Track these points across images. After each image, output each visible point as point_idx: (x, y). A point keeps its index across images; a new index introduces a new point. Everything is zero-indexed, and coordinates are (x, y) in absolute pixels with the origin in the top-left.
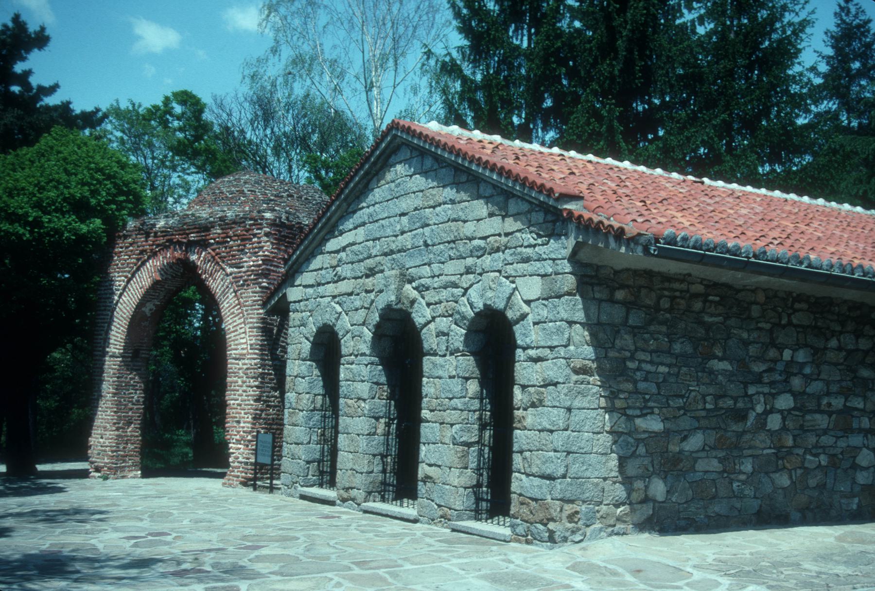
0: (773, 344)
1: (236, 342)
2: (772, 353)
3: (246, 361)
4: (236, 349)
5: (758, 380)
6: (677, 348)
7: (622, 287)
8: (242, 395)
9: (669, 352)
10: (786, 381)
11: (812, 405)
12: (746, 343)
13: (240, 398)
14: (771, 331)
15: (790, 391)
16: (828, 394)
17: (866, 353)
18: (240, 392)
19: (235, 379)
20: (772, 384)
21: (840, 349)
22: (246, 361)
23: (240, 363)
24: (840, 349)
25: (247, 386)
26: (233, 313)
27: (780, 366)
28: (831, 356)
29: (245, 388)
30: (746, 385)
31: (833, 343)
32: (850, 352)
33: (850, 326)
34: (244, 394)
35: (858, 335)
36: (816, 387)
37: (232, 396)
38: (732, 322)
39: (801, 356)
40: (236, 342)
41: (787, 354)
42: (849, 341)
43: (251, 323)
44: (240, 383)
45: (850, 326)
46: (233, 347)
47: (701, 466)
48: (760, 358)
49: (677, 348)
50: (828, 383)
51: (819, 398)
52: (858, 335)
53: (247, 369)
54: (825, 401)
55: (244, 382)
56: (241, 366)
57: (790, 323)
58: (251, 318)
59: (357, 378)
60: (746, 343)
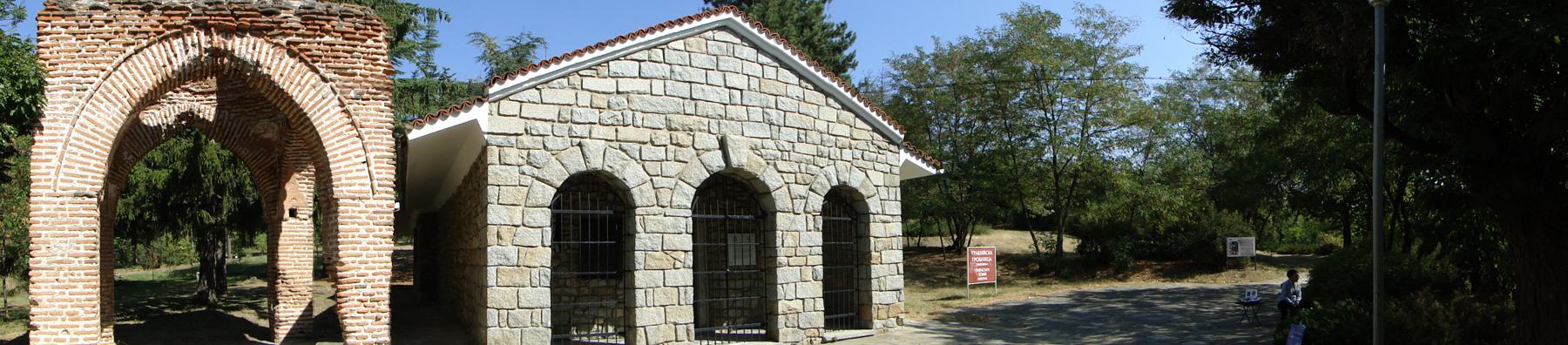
1: (349, 175)
3: (374, 202)
8: (368, 249)
13: (365, 253)
18: (364, 244)
19: (356, 226)
22: (374, 202)
25: (374, 236)
26: (338, 135)
29: (371, 239)
34: (372, 246)
37: (350, 252)
40: (349, 175)
43: (378, 150)
53: (375, 212)
56: (362, 207)
58: (376, 144)
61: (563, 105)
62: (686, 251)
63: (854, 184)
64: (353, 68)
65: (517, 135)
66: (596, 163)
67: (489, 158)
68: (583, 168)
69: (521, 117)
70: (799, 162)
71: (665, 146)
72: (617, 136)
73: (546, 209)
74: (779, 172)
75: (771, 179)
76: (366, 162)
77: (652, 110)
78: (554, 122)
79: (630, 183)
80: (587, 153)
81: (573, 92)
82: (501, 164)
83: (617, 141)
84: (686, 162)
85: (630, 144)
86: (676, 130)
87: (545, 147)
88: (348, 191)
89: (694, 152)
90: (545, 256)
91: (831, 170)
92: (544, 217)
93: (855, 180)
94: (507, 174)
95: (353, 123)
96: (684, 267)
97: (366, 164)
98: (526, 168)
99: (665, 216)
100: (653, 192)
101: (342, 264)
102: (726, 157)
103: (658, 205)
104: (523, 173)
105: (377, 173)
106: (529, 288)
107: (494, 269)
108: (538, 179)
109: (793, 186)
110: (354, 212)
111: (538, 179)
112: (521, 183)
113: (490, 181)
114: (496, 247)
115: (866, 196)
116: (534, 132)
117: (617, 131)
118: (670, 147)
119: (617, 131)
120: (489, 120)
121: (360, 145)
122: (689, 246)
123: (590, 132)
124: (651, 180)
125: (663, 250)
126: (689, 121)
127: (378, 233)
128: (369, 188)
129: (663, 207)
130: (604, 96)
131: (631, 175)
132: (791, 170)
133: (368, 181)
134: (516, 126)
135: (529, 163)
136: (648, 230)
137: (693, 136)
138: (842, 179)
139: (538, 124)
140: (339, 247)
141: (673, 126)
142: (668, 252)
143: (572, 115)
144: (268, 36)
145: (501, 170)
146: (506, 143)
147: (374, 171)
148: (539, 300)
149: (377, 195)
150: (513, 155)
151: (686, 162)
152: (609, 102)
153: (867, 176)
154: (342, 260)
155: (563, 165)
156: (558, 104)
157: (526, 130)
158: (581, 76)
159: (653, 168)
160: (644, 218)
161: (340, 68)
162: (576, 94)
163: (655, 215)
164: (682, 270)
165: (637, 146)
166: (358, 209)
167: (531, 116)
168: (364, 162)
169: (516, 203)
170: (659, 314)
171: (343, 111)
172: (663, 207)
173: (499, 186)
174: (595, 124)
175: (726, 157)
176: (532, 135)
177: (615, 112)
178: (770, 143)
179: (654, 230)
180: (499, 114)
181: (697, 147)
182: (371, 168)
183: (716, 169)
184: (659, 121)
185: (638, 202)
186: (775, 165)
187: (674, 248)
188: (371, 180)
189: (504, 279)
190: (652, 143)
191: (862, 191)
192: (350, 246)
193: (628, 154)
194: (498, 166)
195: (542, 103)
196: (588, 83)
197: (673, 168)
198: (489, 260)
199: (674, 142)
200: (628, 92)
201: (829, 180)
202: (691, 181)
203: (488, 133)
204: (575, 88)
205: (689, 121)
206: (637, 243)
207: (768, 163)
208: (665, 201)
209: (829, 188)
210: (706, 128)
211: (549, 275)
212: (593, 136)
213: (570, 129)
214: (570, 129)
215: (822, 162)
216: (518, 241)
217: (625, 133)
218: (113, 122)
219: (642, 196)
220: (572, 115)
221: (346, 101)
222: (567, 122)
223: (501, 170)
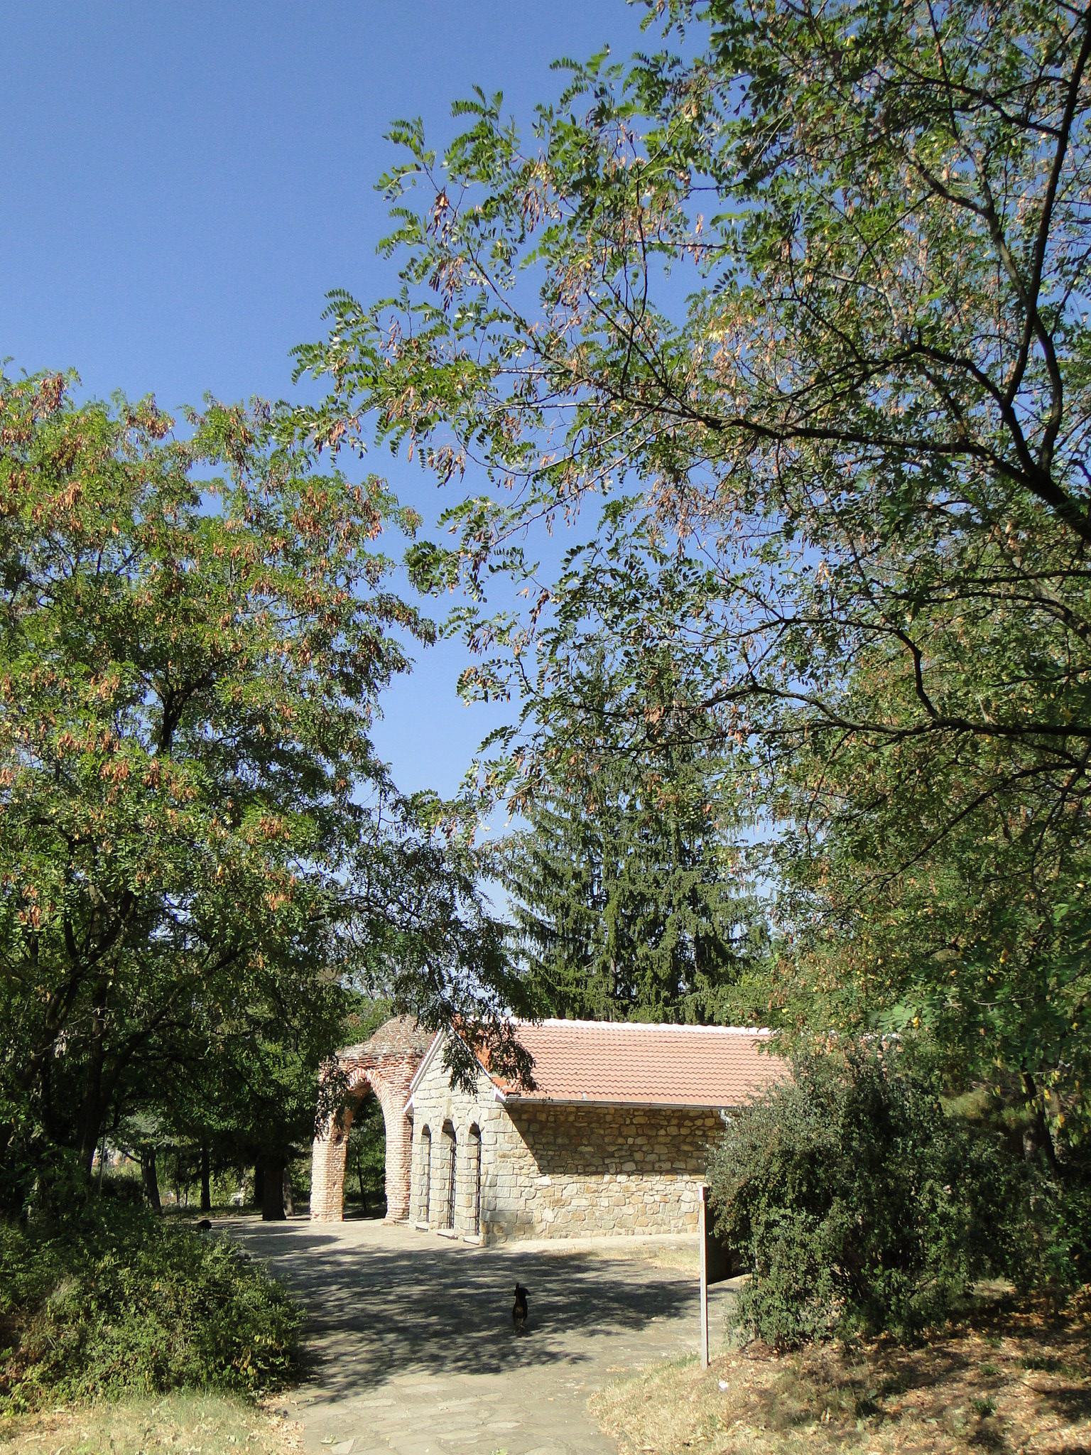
0: (620, 1135)
2: (620, 1140)
5: (612, 1155)
6: (559, 1141)
7: (526, 1112)
9: (555, 1144)
10: (631, 1155)
11: (649, 1167)
12: (603, 1136)
14: (619, 1128)
15: (633, 1161)
16: (660, 1161)
17: (686, 1136)
20: (620, 1157)
21: (667, 1135)
24: (667, 1135)
27: (625, 1147)
28: (661, 1139)
30: (603, 1159)
31: (662, 1132)
32: (674, 1137)
33: (674, 1122)
35: (679, 1126)
36: (652, 1157)
38: (593, 1125)
39: (639, 1141)
41: (630, 1141)
42: (673, 1130)
45: (674, 1122)
47: (575, 1202)
48: (613, 1144)
49: (559, 1141)
50: (659, 1155)
51: (654, 1164)
52: (679, 1126)
54: (657, 1165)
57: (632, 1123)
60: (603, 1136)
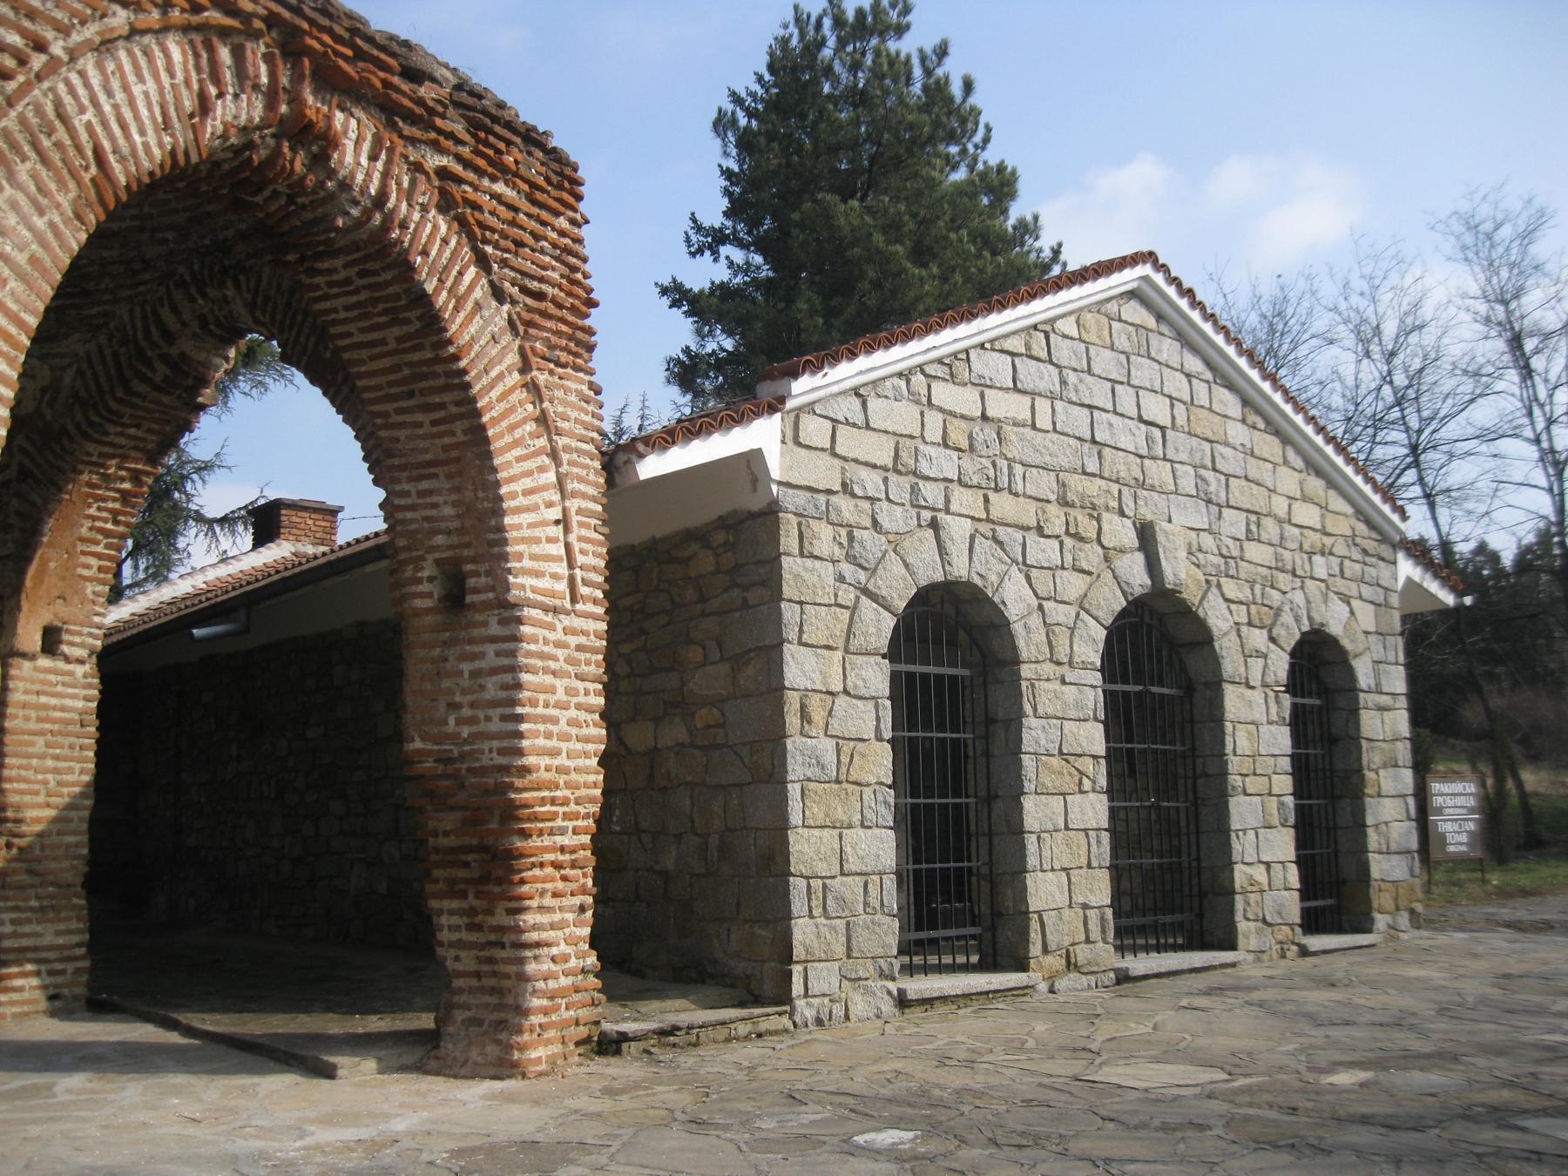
4: (538, 574)
23: (559, 627)
29: (573, 713)
37: (541, 742)
44: (561, 695)
46: (527, 563)
53: (580, 648)
55: (570, 692)
56: (558, 635)
59: (1072, 714)
61: (901, 435)
62: (1094, 757)
63: (1335, 629)
64: (541, 280)
65: (829, 492)
66: (960, 568)
67: (782, 540)
68: (939, 577)
69: (835, 455)
70: (1252, 583)
71: (1057, 537)
72: (987, 511)
73: (879, 659)
74: (1227, 600)
75: (1217, 617)
76: (564, 522)
77: (1037, 462)
78: (886, 469)
79: (1013, 611)
80: (948, 544)
81: (915, 410)
82: (802, 554)
83: (988, 520)
84: (1089, 573)
85: (1009, 530)
86: (1072, 506)
87: (875, 523)
88: (534, 590)
89: (1100, 551)
90: (879, 763)
91: (1298, 597)
92: (876, 677)
93: (1335, 619)
94: (815, 579)
95: (542, 420)
96: (1094, 790)
97: (561, 527)
98: (847, 569)
99: (1063, 682)
100: (1043, 631)
101: (525, 770)
102: (1153, 565)
103: (1051, 660)
104: (841, 578)
105: (581, 552)
106: (861, 832)
107: (797, 786)
108: (866, 591)
109: (1244, 629)
110: (546, 641)
111: (866, 591)
112: (840, 600)
113: (788, 590)
114: (799, 739)
115: (1351, 654)
116: (858, 491)
117: (986, 500)
118: (1069, 542)
119: (986, 500)
120: (782, 454)
121: (551, 477)
122: (1100, 747)
123: (947, 501)
124: (1041, 607)
125: (1061, 752)
126: (1094, 487)
127: (581, 699)
128: (562, 587)
129: (1059, 663)
130: (963, 424)
131: (1014, 598)
132: (1241, 597)
133: (562, 569)
134: (824, 473)
135: (852, 559)
136: (1040, 711)
137: (1098, 520)
138: (1318, 618)
139: (863, 473)
140: (524, 727)
141: (1071, 497)
142: (1071, 759)
143: (917, 460)
144: (401, 136)
145: (806, 569)
146: (811, 511)
147: (577, 546)
148: (878, 856)
149: (579, 607)
150: (824, 538)
151: (1089, 573)
152: (970, 437)
153: (1352, 612)
154: (530, 760)
155: (906, 565)
156: (895, 434)
157: (844, 485)
158: (927, 376)
159: (1042, 580)
160: (1033, 686)
161: (524, 274)
162: (922, 414)
163: (1048, 680)
164: (1091, 795)
165: (1018, 535)
166: (552, 636)
167: (851, 455)
168: (557, 522)
169: (831, 643)
170: (1060, 887)
171: (525, 385)
172: (1059, 663)
173: (801, 603)
174: (951, 481)
175: (1153, 565)
176: (853, 495)
177: (984, 461)
178: (1208, 541)
179: (1050, 711)
180: (798, 444)
181: (1106, 543)
182: (572, 538)
183: (1138, 591)
184: (1044, 485)
185: (1024, 655)
186: (1219, 586)
187: (1079, 751)
188: (571, 566)
189: (817, 812)
190: (1040, 531)
191: (1346, 643)
192: (541, 727)
193: (1004, 550)
194: (799, 560)
195: (868, 427)
196: (944, 394)
197: (1073, 585)
198: (790, 768)
199: (1072, 531)
200: (1000, 421)
201: (1297, 619)
202: (1100, 614)
203: (780, 483)
204: (917, 402)
205: (1094, 487)
206: (1025, 736)
207: (1207, 582)
208: (1062, 653)
209: (1298, 636)
210: (1115, 504)
211: (892, 801)
212: (953, 508)
213: (914, 490)
214: (914, 490)
215: (1283, 580)
216: (836, 728)
217: (1003, 505)
218: (50, 236)
219: (1029, 640)
220: (917, 460)
221: (534, 360)
222: (907, 474)
223: (806, 569)
